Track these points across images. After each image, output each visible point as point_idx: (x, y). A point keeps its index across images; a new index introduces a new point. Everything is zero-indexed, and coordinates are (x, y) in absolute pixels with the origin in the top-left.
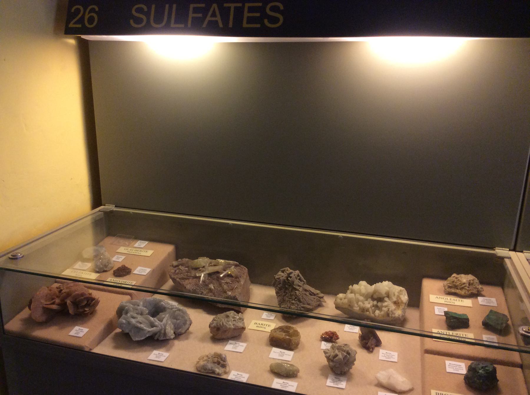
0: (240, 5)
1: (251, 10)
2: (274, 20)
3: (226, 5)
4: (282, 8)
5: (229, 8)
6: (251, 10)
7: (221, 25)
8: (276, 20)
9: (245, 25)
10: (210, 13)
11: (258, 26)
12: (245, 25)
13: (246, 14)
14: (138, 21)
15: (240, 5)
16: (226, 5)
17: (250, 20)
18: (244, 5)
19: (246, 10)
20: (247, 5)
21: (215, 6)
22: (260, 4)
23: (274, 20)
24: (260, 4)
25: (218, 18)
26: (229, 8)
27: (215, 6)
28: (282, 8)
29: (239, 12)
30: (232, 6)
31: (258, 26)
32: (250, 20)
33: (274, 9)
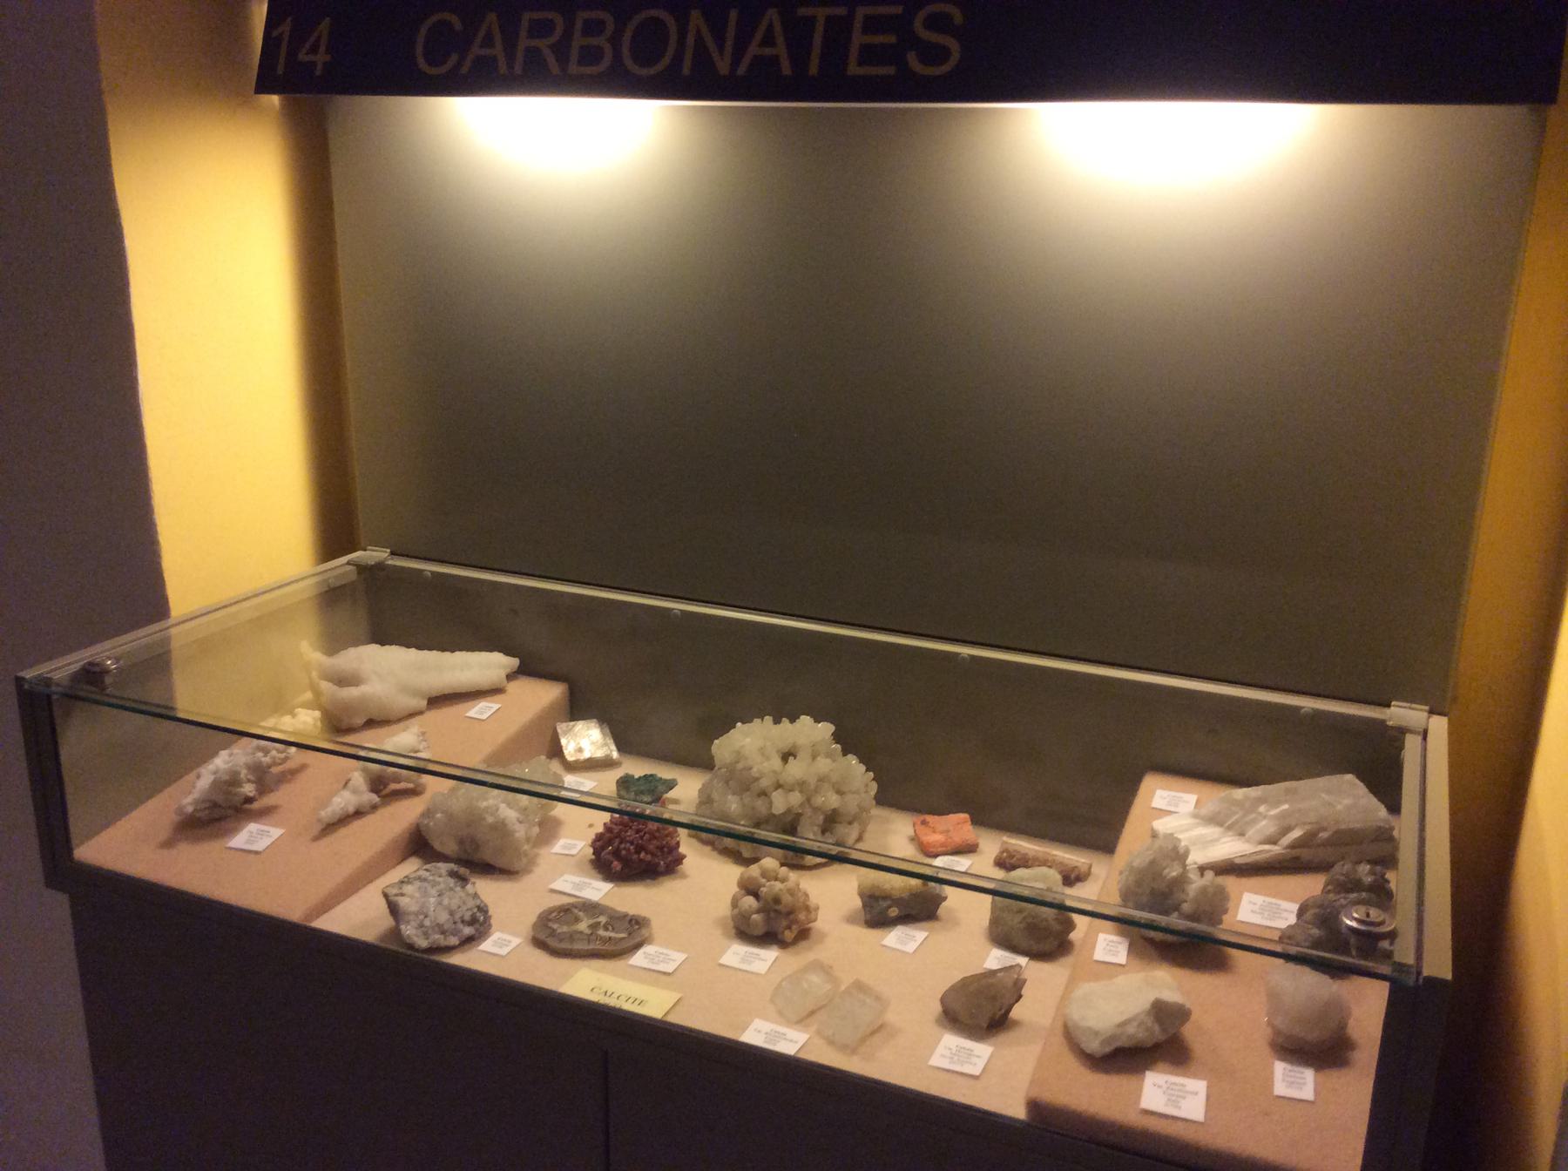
0: (841, 11)
1: (872, 25)
2: (935, 55)
3: (803, 11)
4: (958, 17)
5: (811, 20)
6: (872, 25)
7: (786, 69)
8: (941, 54)
9: (853, 69)
10: (759, 36)
11: (890, 70)
12: (853, 69)
13: (858, 39)
14: (590, 56)
15: (841, 11)
16: (803, 11)
17: (869, 55)
18: (851, 16)
19: (858, 25)
20: (861, 12)
21: (772, 15)
22: (897, 10)
23: (935, 55)
24: (897, 10)
25: (781, 50)
26: (811, 20)
27: (772, 15)
28: (958, 17)
29: (838, 31)
30: (821, 13)
31: (890, 70)
32: (869, 55)
33: (934, 23)
